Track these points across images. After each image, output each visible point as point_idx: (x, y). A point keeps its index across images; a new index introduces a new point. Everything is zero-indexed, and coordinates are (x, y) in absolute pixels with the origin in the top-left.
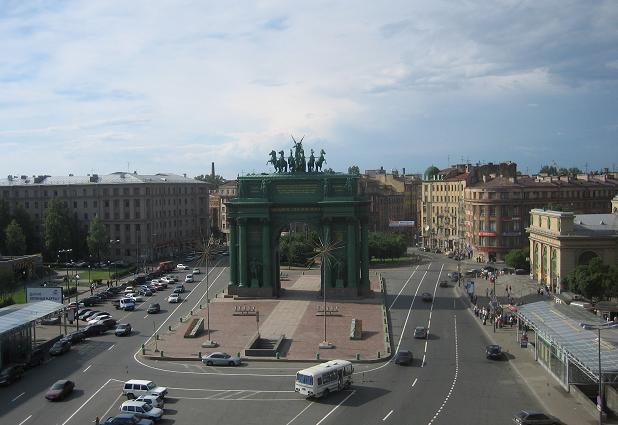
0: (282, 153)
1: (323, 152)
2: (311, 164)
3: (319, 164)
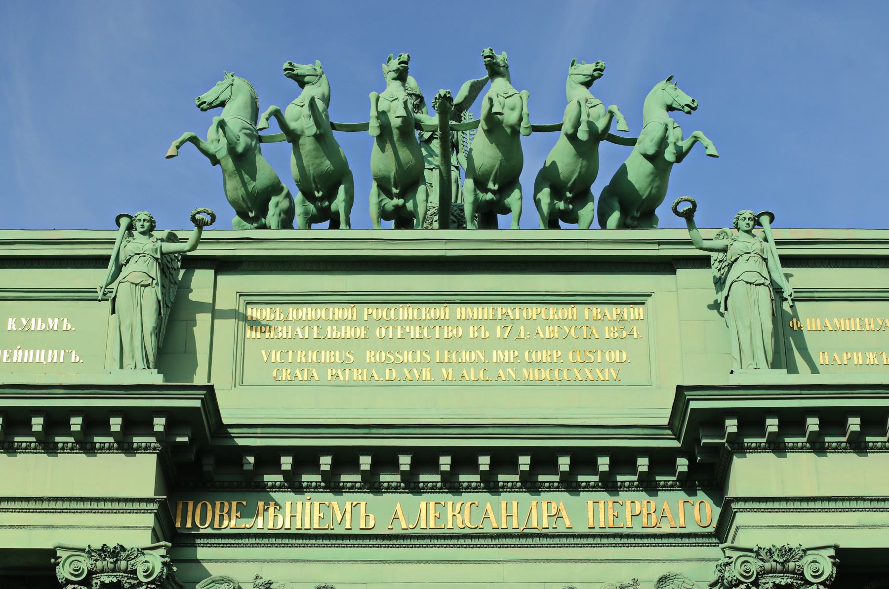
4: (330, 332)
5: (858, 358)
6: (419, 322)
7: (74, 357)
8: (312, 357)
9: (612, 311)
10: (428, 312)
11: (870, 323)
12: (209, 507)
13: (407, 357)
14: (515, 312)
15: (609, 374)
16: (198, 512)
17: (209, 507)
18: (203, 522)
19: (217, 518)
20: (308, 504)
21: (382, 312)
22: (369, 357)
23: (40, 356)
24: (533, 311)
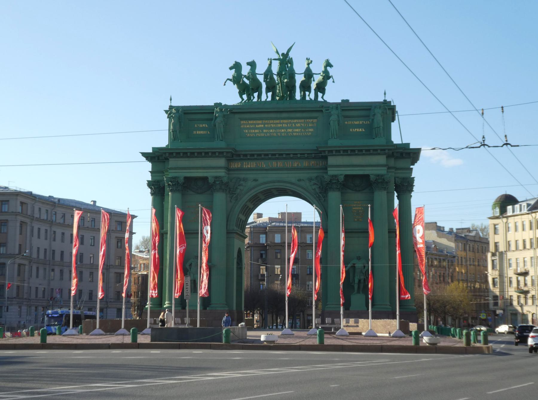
0: (252, 64)
1: (328, 64)
2: (305, 87)
3: (321, 88)
4: (257, 126)
5: (358, 130)
6: (274, 124)
7: (208, 133)
8: (253, 131)
11: (361, 123)
12: (235, 163)
13: (271, 131)
14: (292, 121)
16: (233, 165)
17: (235, 163)
18: (234, 166)
19: (237, 166)
20: (253, 163)
21: (267, 122)
22: (264, 131)
23: (202, 132)
24: (295, 121)
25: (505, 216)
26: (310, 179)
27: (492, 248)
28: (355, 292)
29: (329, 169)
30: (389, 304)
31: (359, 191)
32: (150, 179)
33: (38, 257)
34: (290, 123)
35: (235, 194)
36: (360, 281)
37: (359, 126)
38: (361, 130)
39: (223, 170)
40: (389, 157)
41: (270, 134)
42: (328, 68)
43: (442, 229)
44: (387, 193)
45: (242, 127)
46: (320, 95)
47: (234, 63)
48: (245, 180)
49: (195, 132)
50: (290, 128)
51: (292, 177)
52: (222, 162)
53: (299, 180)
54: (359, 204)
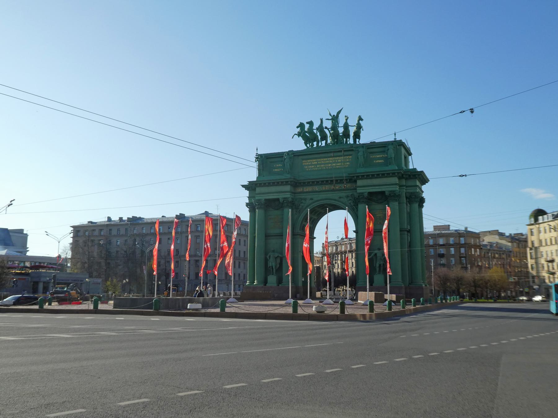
0: (311, 123)
1: (360, 119)
3: (357, 135)
5: (379, 161)
8: (311, 167)
9: (347, 157)
10: (325, 159)
11: (381, 156)
13: (322, 166)
14: (335, 158)
15: (347, 166)
22: (318, 166)
24: (337, 158)
25: (537, 223)
26: (347, 197)
27: (530, 245)
28: (377, 273)
29: (357, 189)
30: (402, 281)
31: (380, 203)
32: (248, 202)
33: (239, 255)
34: (334, 160)
35: (299, 209)
36: (380, 265)
37: (379, 159)
38: (381, 161)
39: (290, 193)
40: (400, 178)
41: (321, 168)
42: (360, 121)
43: (503, 234)
44: (399, 203)
45: (304, 164)
46: (357, 140)
47: (300, 123)
48: (305, 199)
49: (274, 170)
50: (334, 163)
51: (336, 195)
52: (288, 188)
53: (340, 198)
54: (381, 212)
